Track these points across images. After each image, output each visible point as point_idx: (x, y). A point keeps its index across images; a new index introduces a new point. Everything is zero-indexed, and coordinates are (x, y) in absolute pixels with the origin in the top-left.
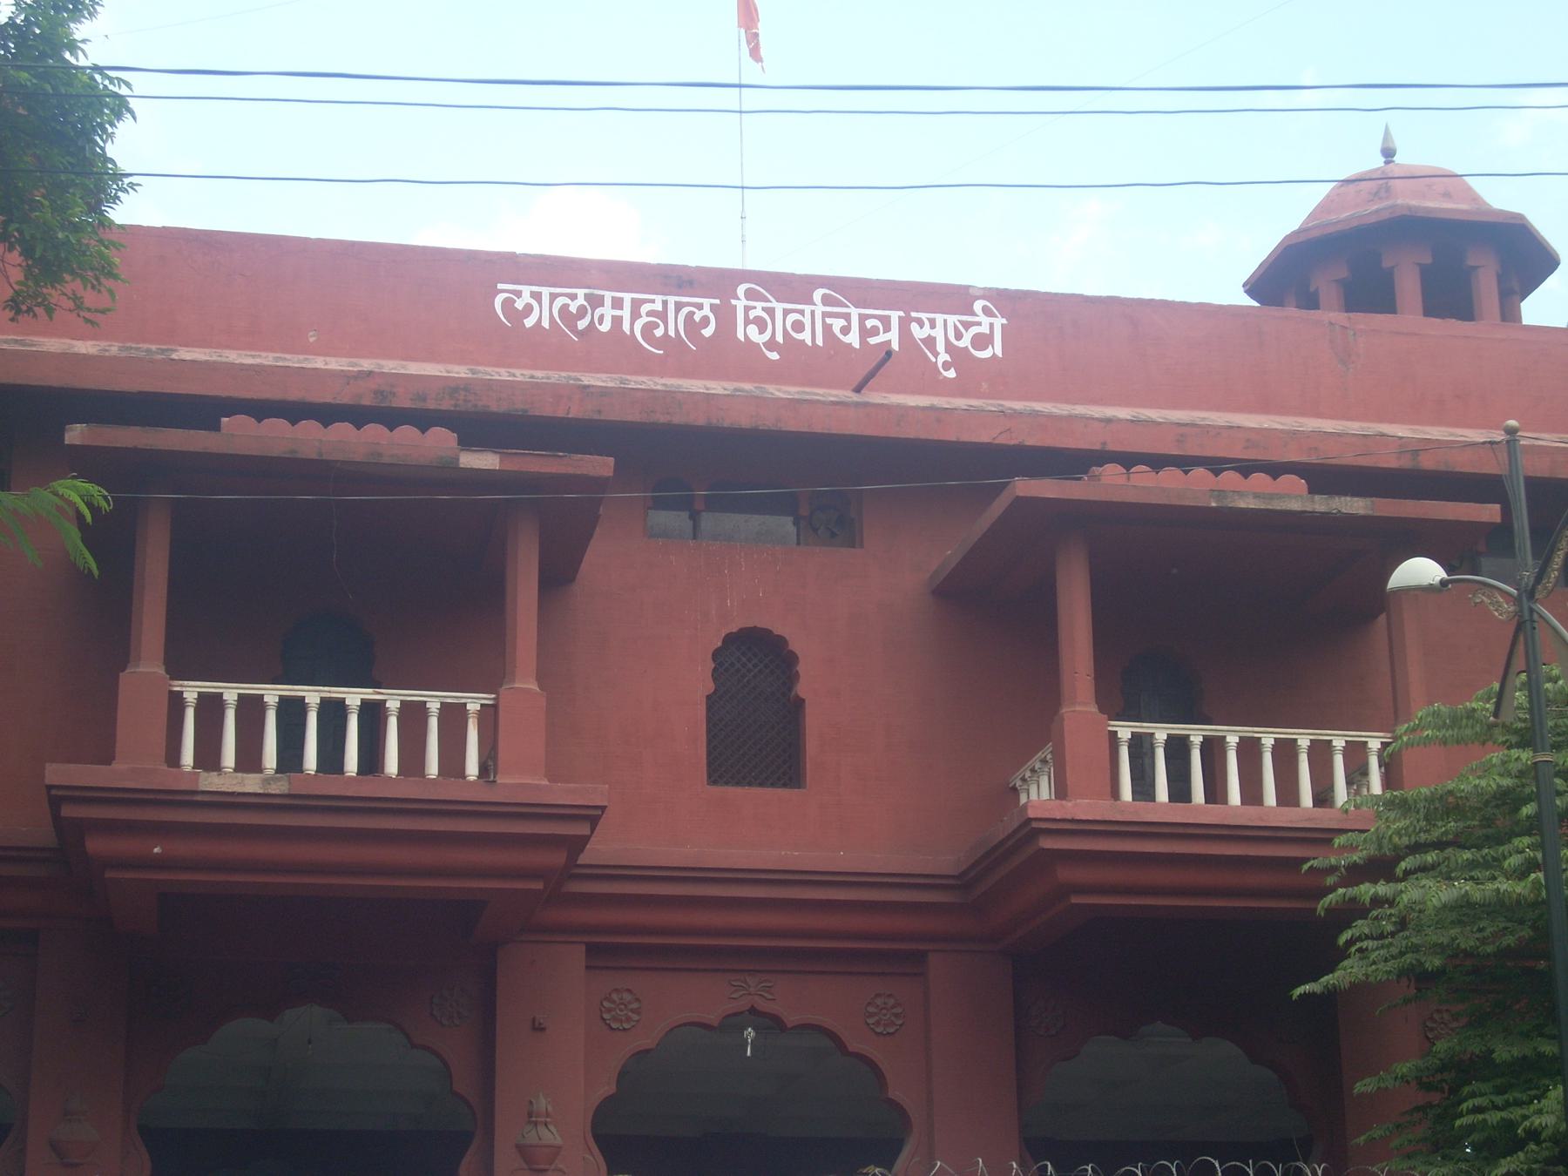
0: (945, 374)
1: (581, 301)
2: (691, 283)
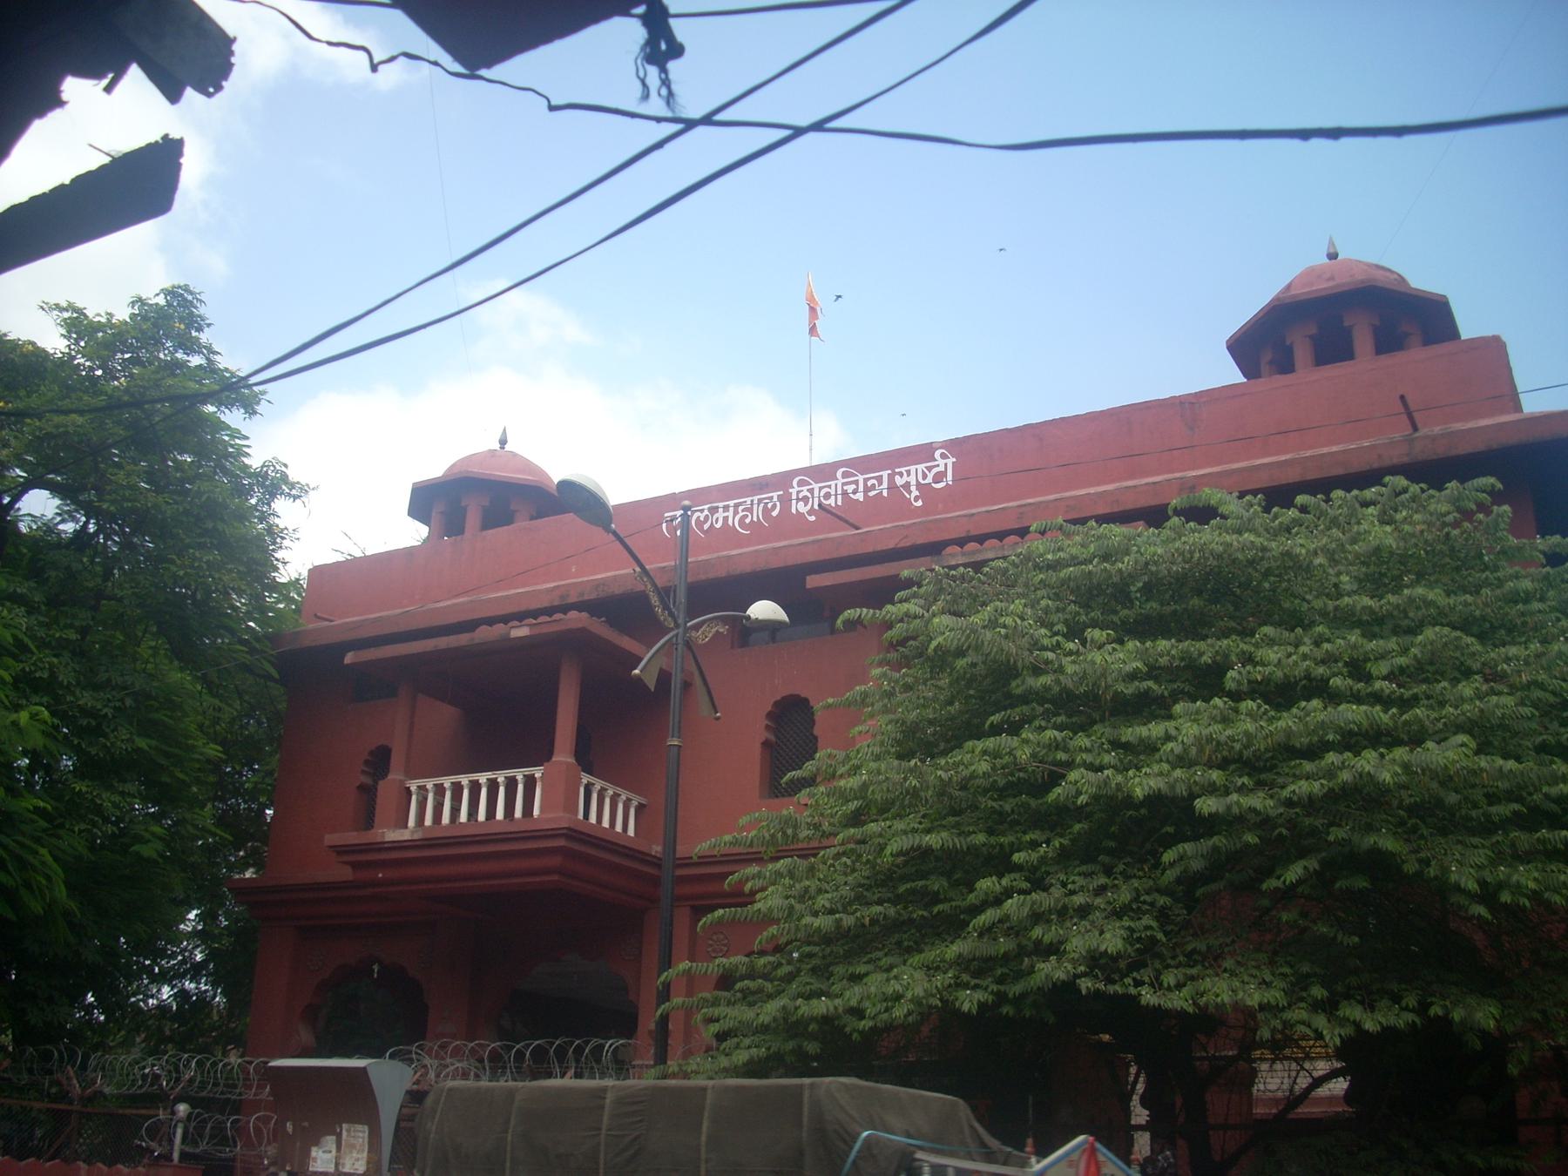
0: (915, 504)
1: (706, 512)
2: (767, 485)
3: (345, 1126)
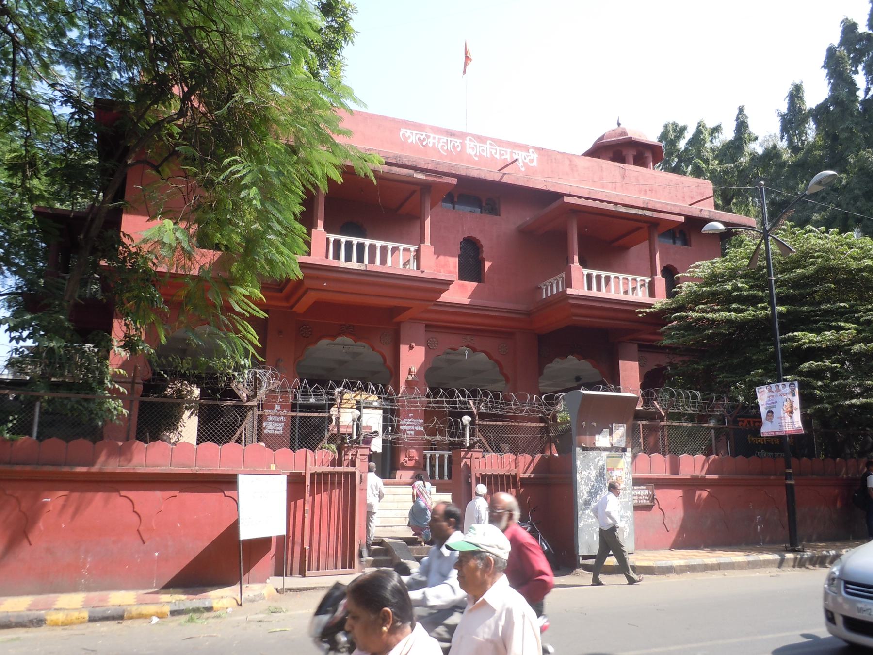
3: (614, 424)
